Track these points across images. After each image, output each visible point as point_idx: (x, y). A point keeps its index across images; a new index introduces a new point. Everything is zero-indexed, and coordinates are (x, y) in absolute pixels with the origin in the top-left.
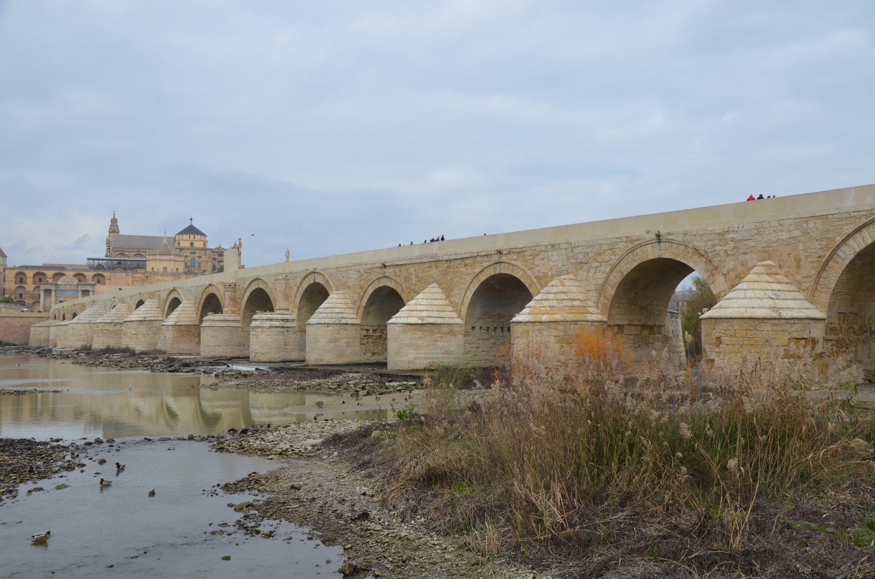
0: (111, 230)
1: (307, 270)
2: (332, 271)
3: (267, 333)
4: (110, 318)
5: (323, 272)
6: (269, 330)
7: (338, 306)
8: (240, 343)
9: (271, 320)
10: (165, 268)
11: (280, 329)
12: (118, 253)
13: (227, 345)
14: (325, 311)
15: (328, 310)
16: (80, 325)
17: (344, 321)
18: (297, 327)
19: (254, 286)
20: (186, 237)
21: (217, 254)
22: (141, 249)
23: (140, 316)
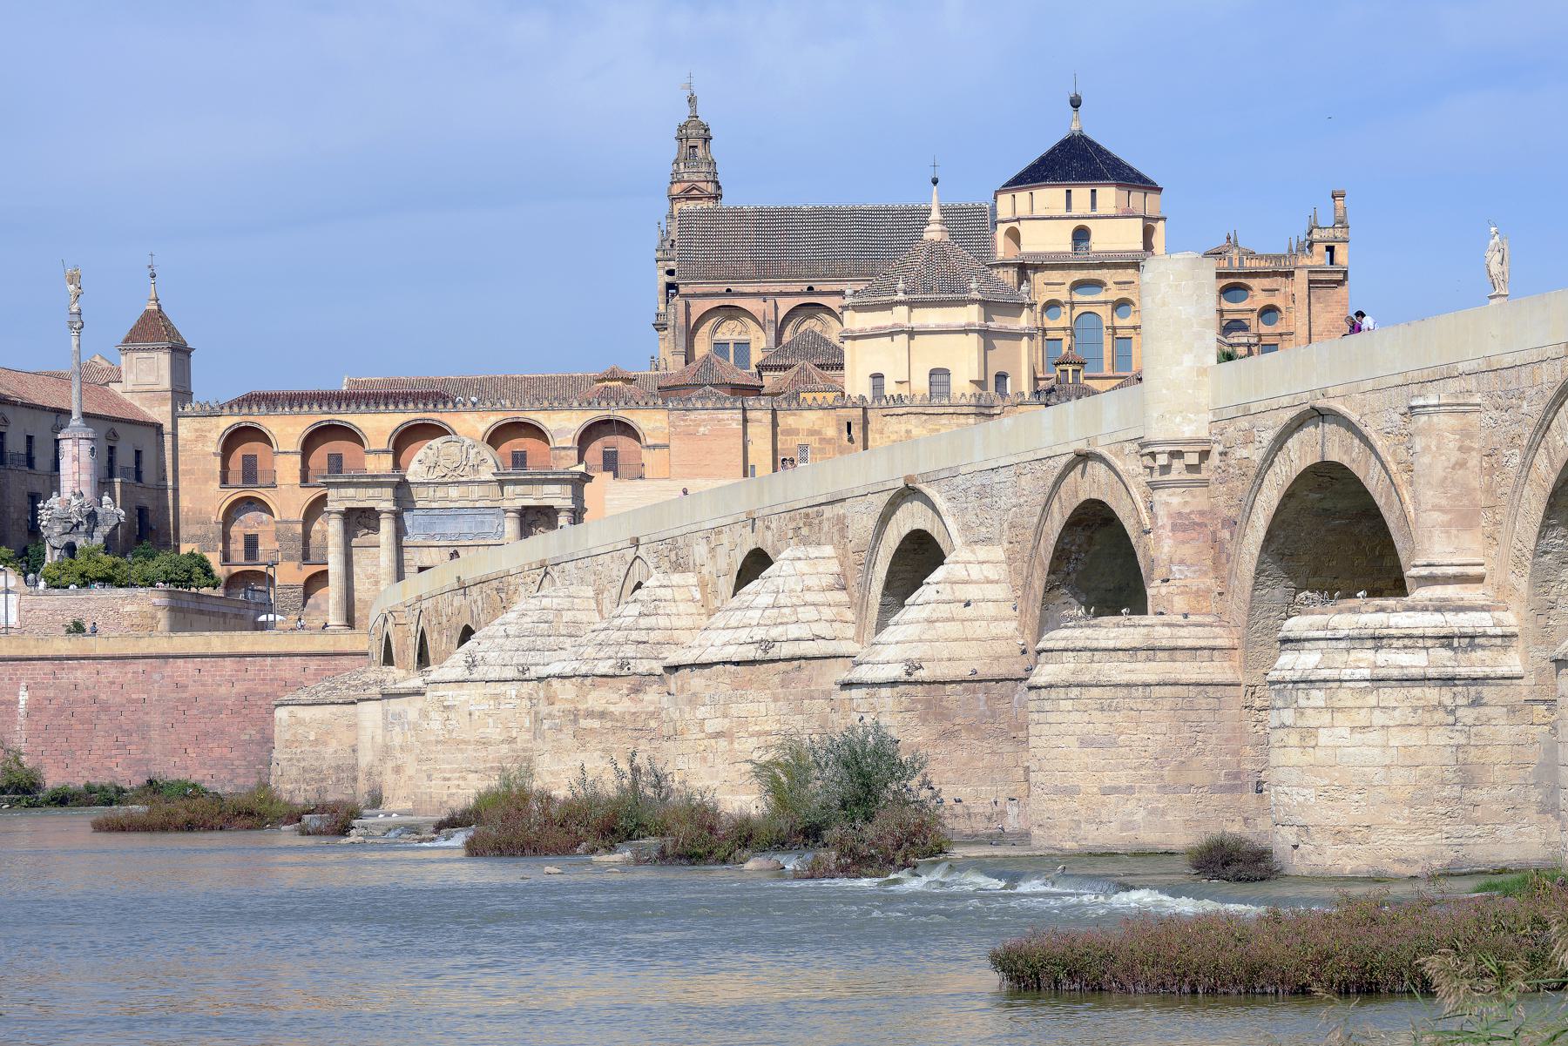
0: (677, 189)
3: (1361, 718)
4: (610, 651)
6: (1372, 700)
8: (1236, 776)
9: (1379, 640)
10: (939, 376)
11: (1432, 694)
13: (1163, 789)
18: (1530, 680)
19: (1301, 454)
20: (1049, 197)
23: (743, 635)
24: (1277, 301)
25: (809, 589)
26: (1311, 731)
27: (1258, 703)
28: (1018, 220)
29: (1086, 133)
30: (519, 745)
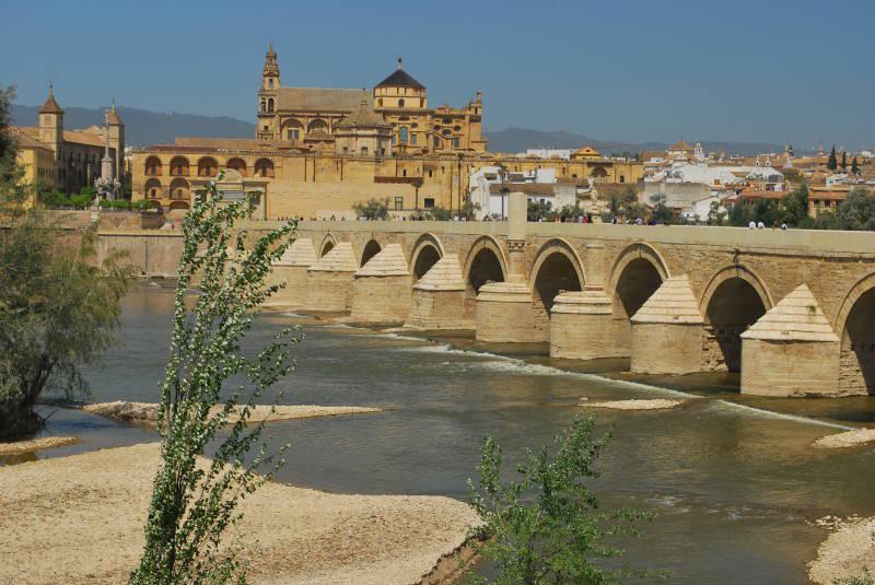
1: (629, 240)
2: (665, 246)
7: (675, 298)
14: (657, 304)
15: (662, 304)
17: (681, 320)
20: (392, 91)
22: (322, 112)
24: (460, 125)
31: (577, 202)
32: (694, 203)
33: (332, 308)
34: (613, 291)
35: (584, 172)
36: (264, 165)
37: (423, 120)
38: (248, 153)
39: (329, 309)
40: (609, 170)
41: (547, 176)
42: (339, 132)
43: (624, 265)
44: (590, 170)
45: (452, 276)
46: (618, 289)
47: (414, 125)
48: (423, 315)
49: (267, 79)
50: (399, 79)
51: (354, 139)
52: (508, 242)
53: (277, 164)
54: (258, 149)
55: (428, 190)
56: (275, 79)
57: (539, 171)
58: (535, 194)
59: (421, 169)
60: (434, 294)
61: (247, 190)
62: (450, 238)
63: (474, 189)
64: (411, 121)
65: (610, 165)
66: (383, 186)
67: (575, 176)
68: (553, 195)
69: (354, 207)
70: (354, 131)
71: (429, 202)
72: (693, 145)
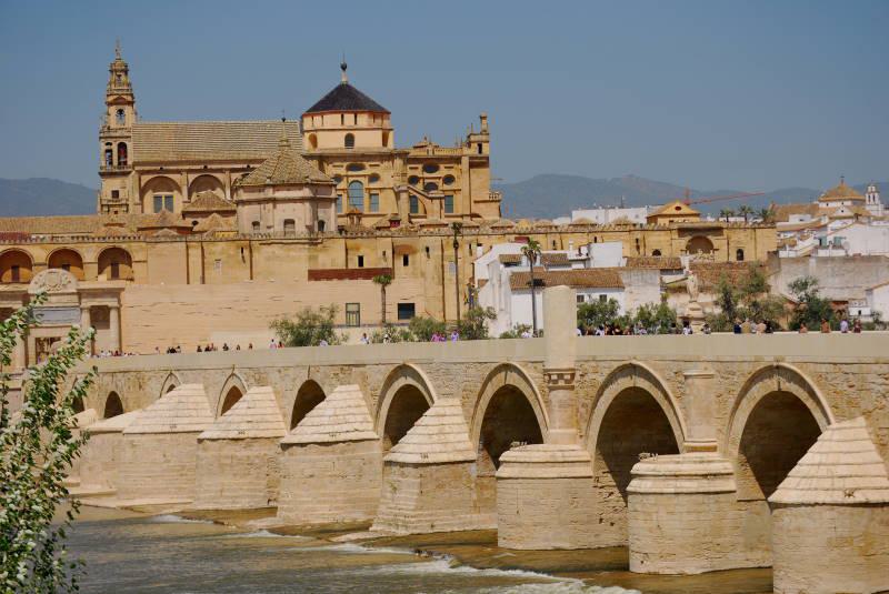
0: (111, 99)
2: (823, 369)
4: (235, 426)
5: (801, 368)
12: (151, 177)
14: (813, 470)
15: (823, 471)
16: (153, 437)
17: (859, 497)
20: (332, 120)
21: (420, 166)
22: (212, 162)
23: (321, 429)
24: (452, 172)
25: (350, 407)
26: (649, 514)
27: (599, 485)
28: (316, 130)
29: (350, 83)
30: (171, 464)
31: (664, 299)
32: (870, 291)
33: (244, 504)
34: (735, 451)
35: (673, 246)
36: (114, 259)
37: (386, 169)
38: (84, 239)
39: (238, 506)
40: (715, 241)
41: (608, 255)
42: (244, 196)
43: (753, 404)
44: (684, 241)
45: (451, 438)
46: (744, 448)
47: (374, 178)
48: (404, 509)
49: (113, 110)
50: (343, 100)
51: (270, 206)
52: (547, 373)
53: (136, 257)
54: (103, 231)
55: (401, 290)
56: (128, 110)
57: (594, 246)
58: (589, 286)
59: (389, 253)
60: (421, 471)
61: (88, 303)
62: (444, 371)
63: (483, 282)
64: (369, 171)
65: (718, 230)
66: (323, 284)
67: (657, 253)
68: (620, 287)
69: (274, 325)
70: (270, 193)
71: (406, 310)
72: (863, 189)
